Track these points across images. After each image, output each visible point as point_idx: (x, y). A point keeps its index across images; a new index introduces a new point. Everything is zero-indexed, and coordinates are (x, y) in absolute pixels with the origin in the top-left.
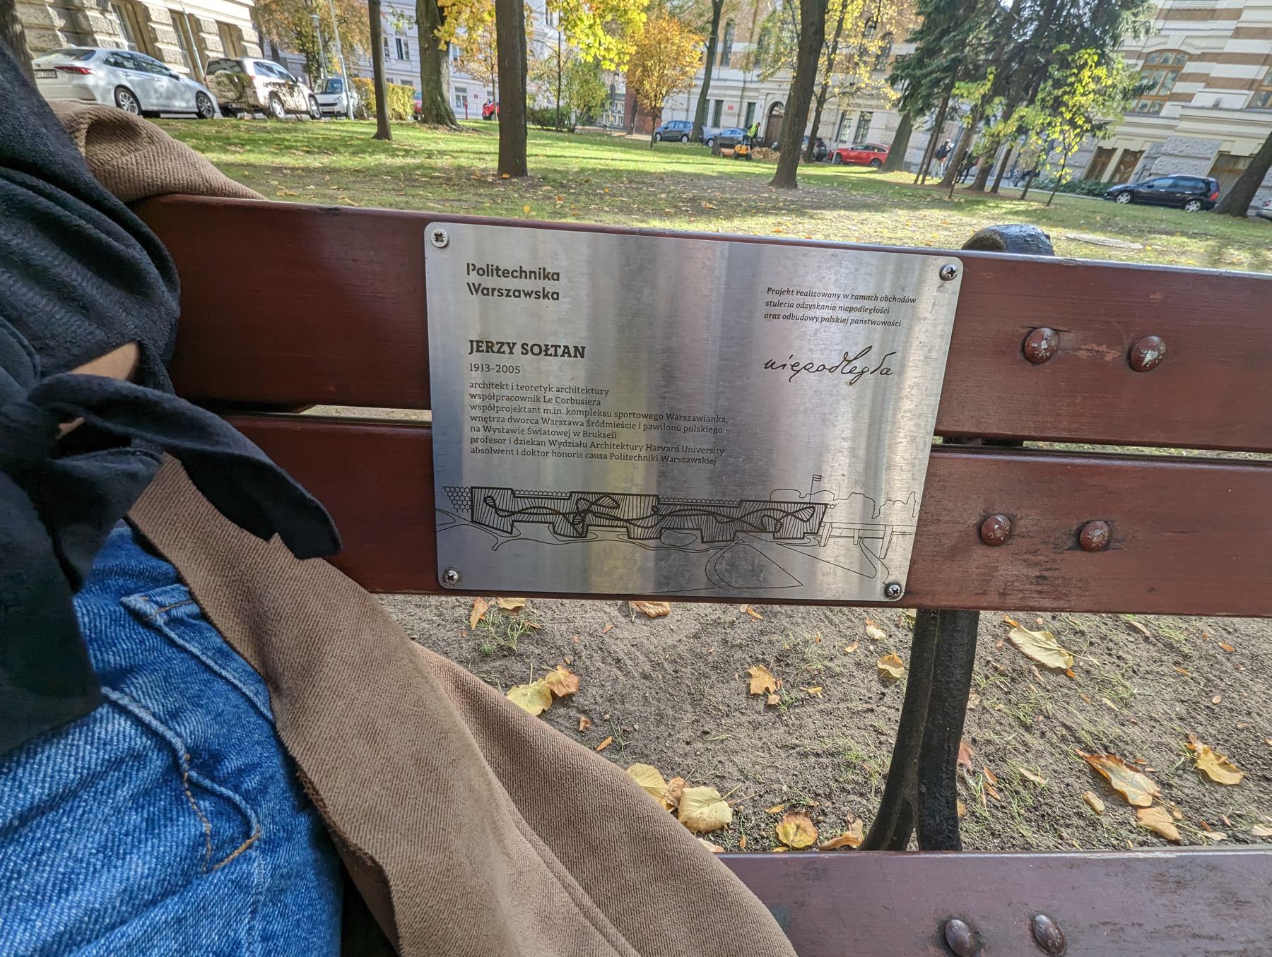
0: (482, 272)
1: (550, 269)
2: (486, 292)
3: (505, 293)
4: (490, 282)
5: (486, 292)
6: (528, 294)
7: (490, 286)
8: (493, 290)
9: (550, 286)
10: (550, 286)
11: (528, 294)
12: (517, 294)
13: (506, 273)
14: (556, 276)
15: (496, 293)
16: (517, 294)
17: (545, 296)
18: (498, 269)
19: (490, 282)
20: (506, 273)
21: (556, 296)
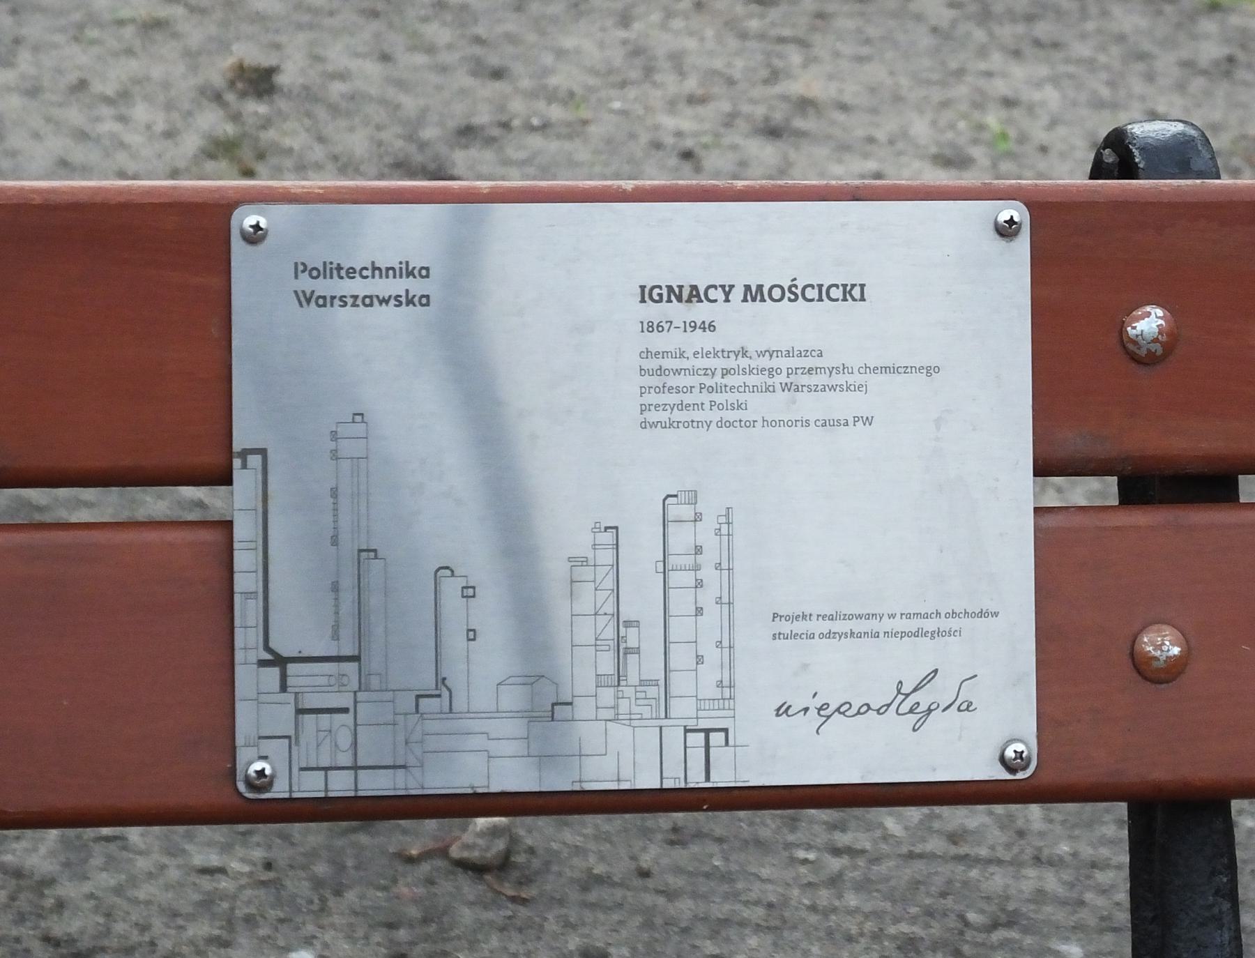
0: (315, 273)
1: (416, 263)
2: (324, 301)
3: (350, 301)
4: (324, 287)
5: (324, 301)
6: (384, 301)
7: (328, 294)
8: (333, 298)
10: (416, 287)
11: (384, 301)
12: (368, 301)
13: (351, 273)
14: (425, 272)
15: (337, 302)
16: (368, 301)
17: (410, 302)
18: (339, 268)
19: (324, 287)
20: (351, 273)
21: (425, 300)
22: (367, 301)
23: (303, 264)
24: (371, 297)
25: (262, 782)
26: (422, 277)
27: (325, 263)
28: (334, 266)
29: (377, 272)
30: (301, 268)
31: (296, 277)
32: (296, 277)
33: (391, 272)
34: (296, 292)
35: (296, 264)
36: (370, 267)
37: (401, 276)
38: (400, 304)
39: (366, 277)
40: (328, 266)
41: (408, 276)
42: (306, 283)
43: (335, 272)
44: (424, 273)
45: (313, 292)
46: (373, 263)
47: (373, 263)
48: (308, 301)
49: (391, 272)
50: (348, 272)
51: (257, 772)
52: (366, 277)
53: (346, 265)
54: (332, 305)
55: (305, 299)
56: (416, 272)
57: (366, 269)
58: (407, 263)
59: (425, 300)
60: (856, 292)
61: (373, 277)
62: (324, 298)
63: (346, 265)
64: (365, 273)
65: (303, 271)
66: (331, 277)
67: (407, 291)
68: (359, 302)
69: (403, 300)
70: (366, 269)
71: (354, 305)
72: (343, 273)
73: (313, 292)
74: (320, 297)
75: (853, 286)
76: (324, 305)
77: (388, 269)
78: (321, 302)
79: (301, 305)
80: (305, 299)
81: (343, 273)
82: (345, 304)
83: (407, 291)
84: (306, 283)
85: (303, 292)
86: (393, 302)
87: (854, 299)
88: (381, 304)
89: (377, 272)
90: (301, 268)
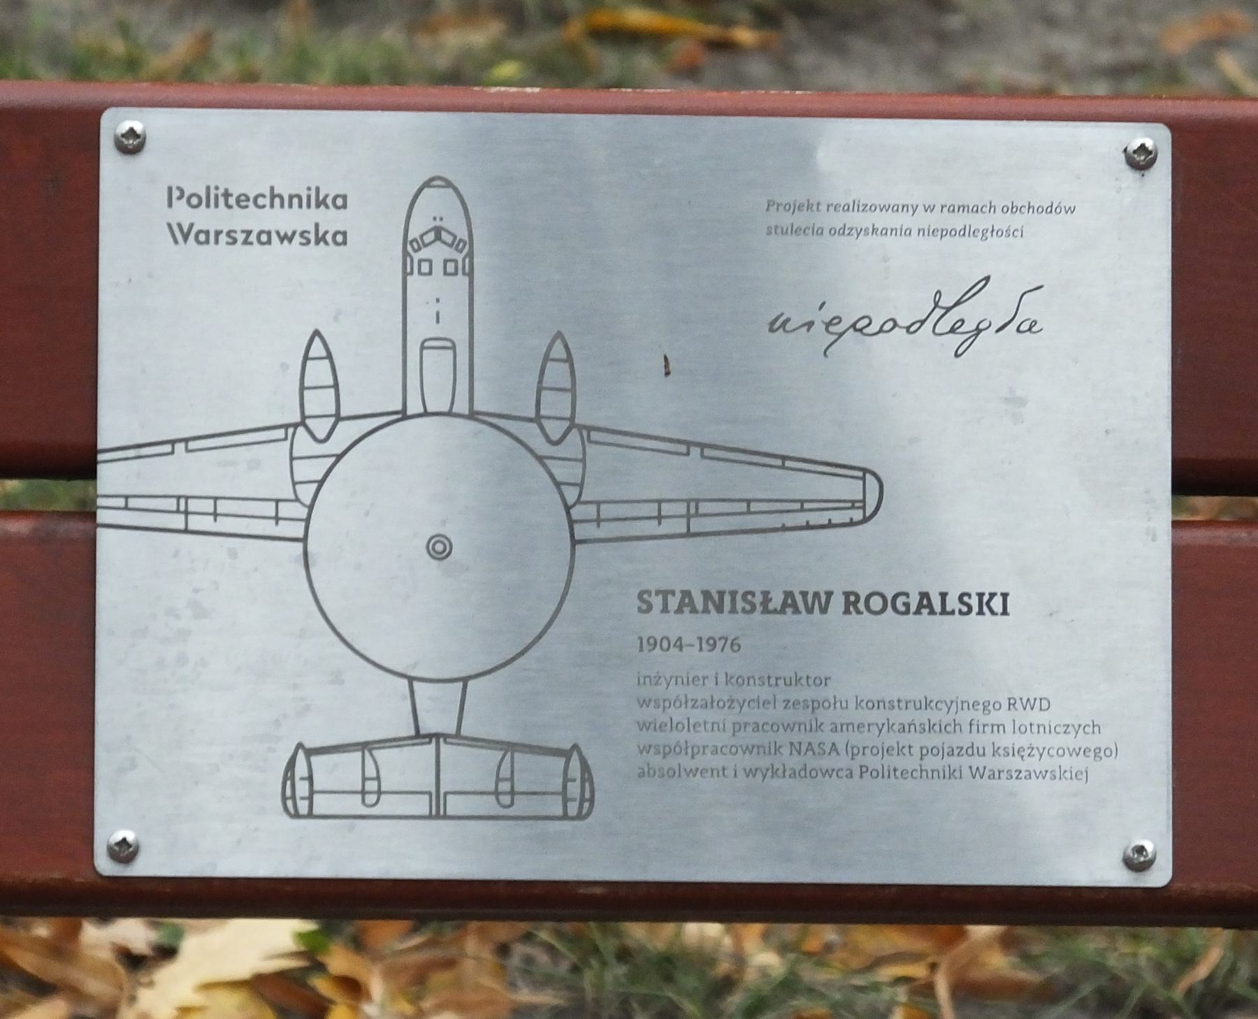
0: (195, 201)
1: (329, 190)
2: (205, 237)
3: (241, 237)
4: (205, 219)
6: (286, 238)
8: (218, 233)
9: (330, 220)
10: (330, 220)
11: (286, 238)
12: (265, 238)
13: (242, 201)
14: (341, 202)
16: (265, 238)
17: (320, 239)
18: (227, 195)
19: (205, 219)
20: (242, 201)
21: (341, 238)
22: (264, 238)
23: (180, 189)
24: (269, 233)
25: (124, 852)
26: (338, 208)
27: (208, 188)
28: (221, 191)
29: (277, 201)
30: (176, 194)
31: (170, 205)
32: (170, 205)
33: (295, 201)
34: (169, 226)
35: (170, 189)
36: (268, 193)
37: (309, 206)
38: (309, 242)
39: (264, 206)
40: (213, 192)
41: (318, 206)
42: (182, 213)
43: (221, 200)
44: (339, 202)
45: (191, 225)
46: (272, 189)
47: (272, 189)
48: (186, 237)
49: (295, 201)
50: (238, 201)
51: (118, 844)
52: (264, 206)
53: (235, 192)
54: (217, 242)
55: (184, 234)
56: (329, 201)
57: (264, 196)
58: (318, 189)
59: (341, 238)
60: (997, 604)
61: (272, 206)
62: (207, 233)
63: (235, 192)
64: (261, 201)
65: (180, 198)
66: (217, 206)
67: (317, 225)
68: (253, 238)
69: (312, 237)
70: (264, 196)
71: (246, 242)
72: (232, 201)
73: (191, 225)
74: (200, 232)
75: (992, 595)
76: (207, 242)
77: (291, 197)
78: (202, 237)
79: (176, 242)
80: (184, 234)
81: (232, 201)
82: (235, 241)
83: (317, 225)
84: (182, 213)
85: (180, 225)
86: (297, 239)
87: (993, 612)
88: (282, 240)
89: (277, 201)
90: (176, 194)
